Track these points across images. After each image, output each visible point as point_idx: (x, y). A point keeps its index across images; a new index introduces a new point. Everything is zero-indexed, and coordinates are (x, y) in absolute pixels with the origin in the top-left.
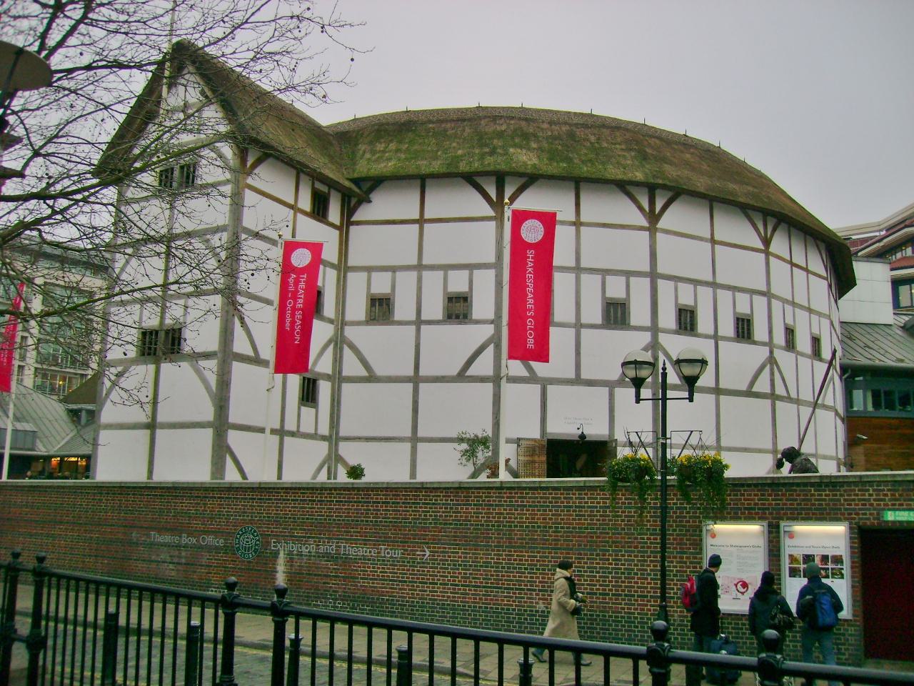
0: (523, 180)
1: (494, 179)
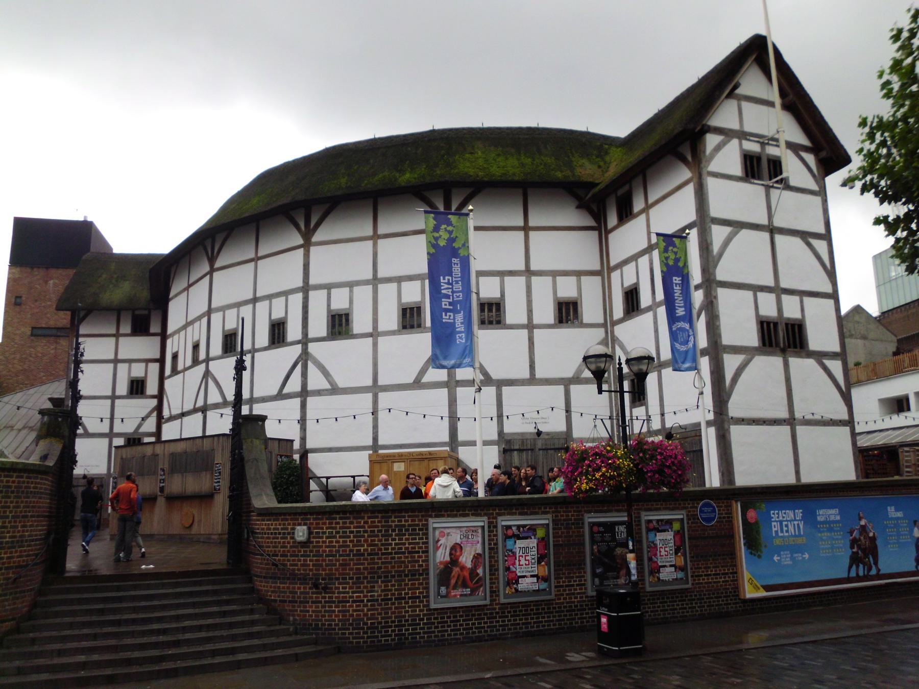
0: (327, 206)
1: (302, 211)
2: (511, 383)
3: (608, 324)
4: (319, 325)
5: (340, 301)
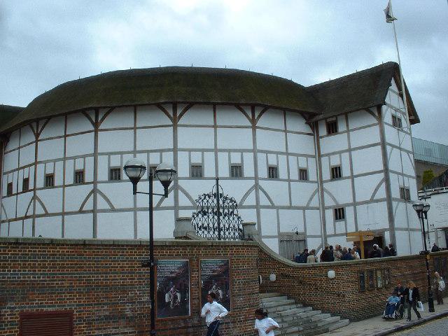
1: (171, 105)
2: (283, 208)
3: (321, 182)
4: (184, 171)
5: (196, 158)
